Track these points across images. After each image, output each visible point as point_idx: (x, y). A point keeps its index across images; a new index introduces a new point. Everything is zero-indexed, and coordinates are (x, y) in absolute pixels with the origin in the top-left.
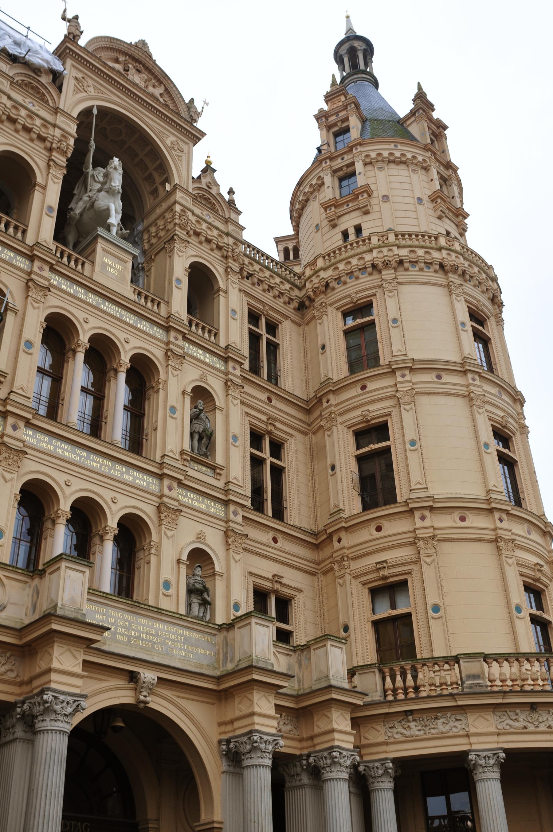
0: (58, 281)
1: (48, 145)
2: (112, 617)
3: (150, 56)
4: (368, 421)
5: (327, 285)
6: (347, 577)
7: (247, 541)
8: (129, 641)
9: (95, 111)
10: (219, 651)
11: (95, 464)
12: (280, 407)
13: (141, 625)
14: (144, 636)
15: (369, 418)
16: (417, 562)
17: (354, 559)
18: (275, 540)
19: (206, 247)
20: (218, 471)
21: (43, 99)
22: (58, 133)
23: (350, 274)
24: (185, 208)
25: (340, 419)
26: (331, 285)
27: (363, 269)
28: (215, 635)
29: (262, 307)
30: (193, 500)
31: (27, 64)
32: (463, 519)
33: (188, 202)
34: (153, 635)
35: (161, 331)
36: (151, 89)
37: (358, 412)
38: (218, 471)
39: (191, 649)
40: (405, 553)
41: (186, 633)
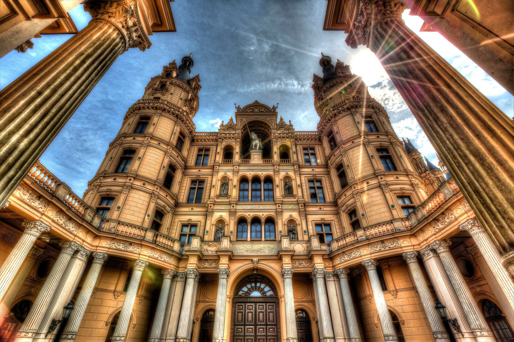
3: (259, 103)
5: (322, 131)
16: (356, 202)
19: (284, 140)
22: (236, 135)
24: (274, 133)
36: (261, 110)
37: (334, 163)
40: (352, 201)
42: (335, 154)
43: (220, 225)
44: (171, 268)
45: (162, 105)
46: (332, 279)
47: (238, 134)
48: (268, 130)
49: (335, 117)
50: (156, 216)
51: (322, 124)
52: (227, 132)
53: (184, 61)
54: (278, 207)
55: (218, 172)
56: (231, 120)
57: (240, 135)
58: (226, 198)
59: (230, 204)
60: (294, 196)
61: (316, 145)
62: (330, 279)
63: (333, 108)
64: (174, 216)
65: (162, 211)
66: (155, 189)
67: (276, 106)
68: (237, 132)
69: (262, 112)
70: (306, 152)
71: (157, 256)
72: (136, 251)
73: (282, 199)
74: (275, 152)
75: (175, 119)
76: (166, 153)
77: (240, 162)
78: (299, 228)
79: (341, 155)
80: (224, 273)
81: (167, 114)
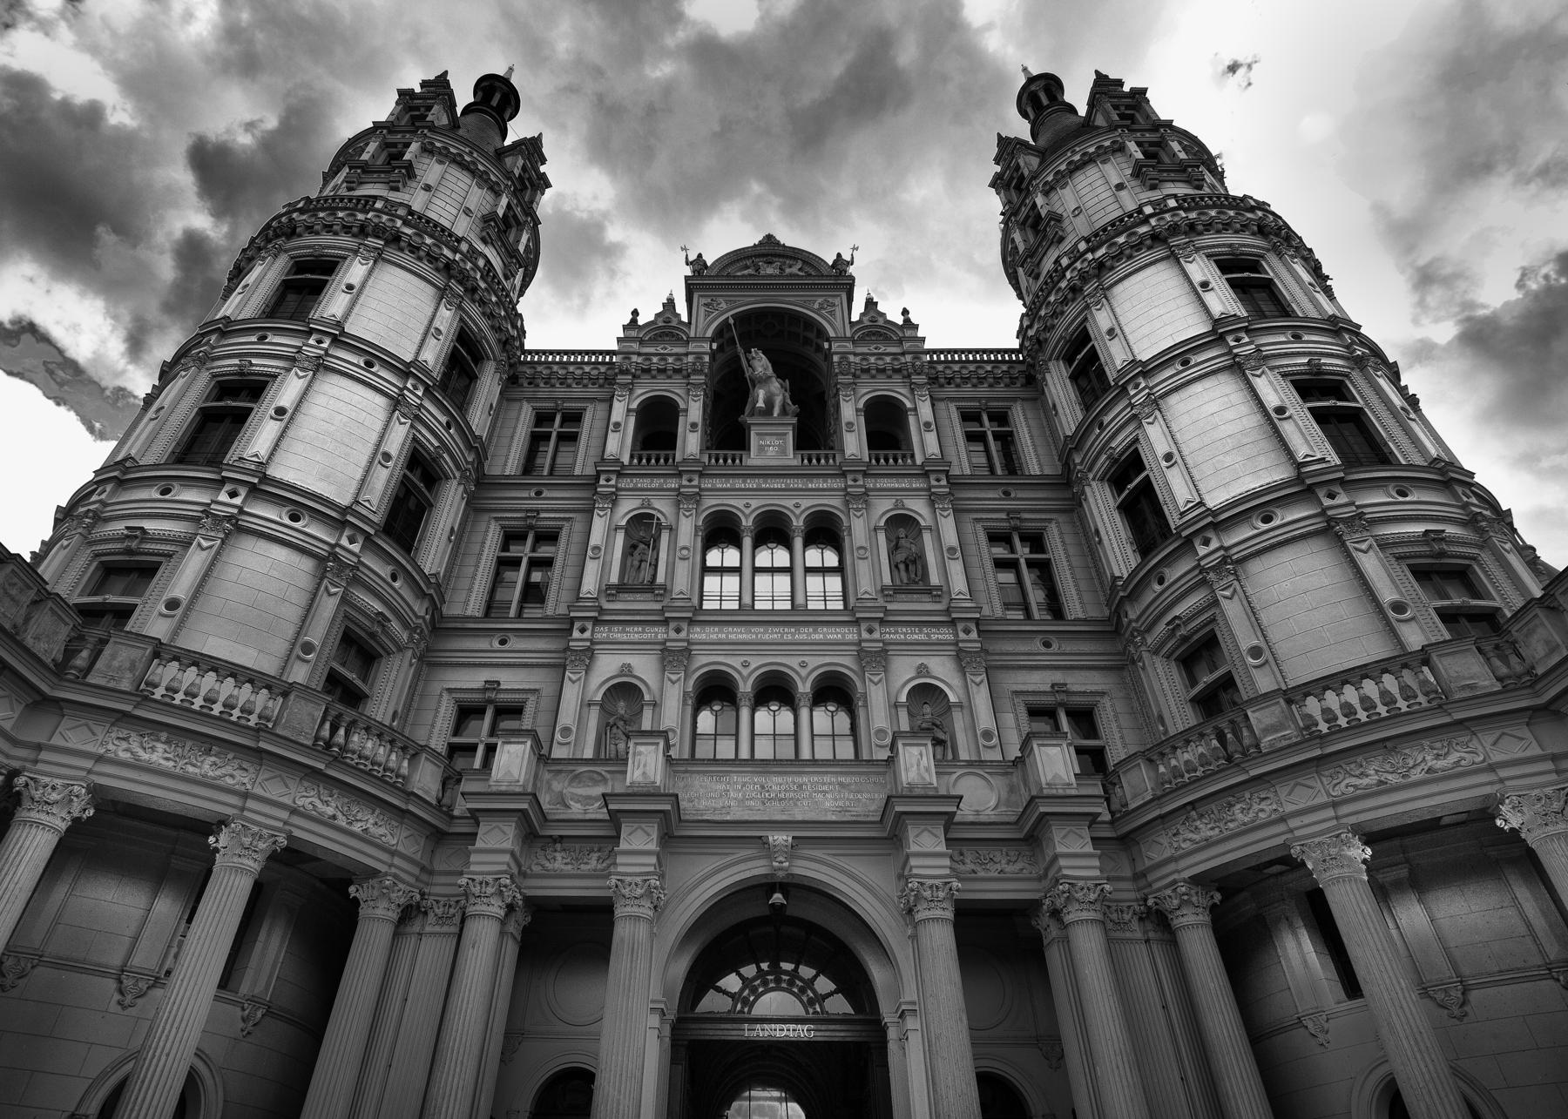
1: (685, 373)
5: (1039, 342)
7: (990, 658)
9: (731, 321)
22: (691, 358)
24: (844, 355)
28: (884, 773)
30: (905, 634)
32: (1267, 519)
33: (849, 346)
36: (788, 271)
39: (851, 797)
41: (842, 779)
43: (622, 707)
44: (393, 870)
45: (385, 218)
47: (699, 356)
48: (819, 348)
52: (651, 350)
53: (483, 89)
54: (865, 635)
56: (670, 304)
57: (707, 359)
58: (649, 596)
59: (666, 622)
60: (930, 591)
61: (1014, 399)
65: (373, 635)
67: (846, 257)
68: (692, 347)
69: (792, 276)
71: (330, 811)
72: (229, 781)
73: (881, 602)
74: (850, 424)
77: (706, 460)
78: (959, 721)
80: (639, 891)
81: (406, 258)
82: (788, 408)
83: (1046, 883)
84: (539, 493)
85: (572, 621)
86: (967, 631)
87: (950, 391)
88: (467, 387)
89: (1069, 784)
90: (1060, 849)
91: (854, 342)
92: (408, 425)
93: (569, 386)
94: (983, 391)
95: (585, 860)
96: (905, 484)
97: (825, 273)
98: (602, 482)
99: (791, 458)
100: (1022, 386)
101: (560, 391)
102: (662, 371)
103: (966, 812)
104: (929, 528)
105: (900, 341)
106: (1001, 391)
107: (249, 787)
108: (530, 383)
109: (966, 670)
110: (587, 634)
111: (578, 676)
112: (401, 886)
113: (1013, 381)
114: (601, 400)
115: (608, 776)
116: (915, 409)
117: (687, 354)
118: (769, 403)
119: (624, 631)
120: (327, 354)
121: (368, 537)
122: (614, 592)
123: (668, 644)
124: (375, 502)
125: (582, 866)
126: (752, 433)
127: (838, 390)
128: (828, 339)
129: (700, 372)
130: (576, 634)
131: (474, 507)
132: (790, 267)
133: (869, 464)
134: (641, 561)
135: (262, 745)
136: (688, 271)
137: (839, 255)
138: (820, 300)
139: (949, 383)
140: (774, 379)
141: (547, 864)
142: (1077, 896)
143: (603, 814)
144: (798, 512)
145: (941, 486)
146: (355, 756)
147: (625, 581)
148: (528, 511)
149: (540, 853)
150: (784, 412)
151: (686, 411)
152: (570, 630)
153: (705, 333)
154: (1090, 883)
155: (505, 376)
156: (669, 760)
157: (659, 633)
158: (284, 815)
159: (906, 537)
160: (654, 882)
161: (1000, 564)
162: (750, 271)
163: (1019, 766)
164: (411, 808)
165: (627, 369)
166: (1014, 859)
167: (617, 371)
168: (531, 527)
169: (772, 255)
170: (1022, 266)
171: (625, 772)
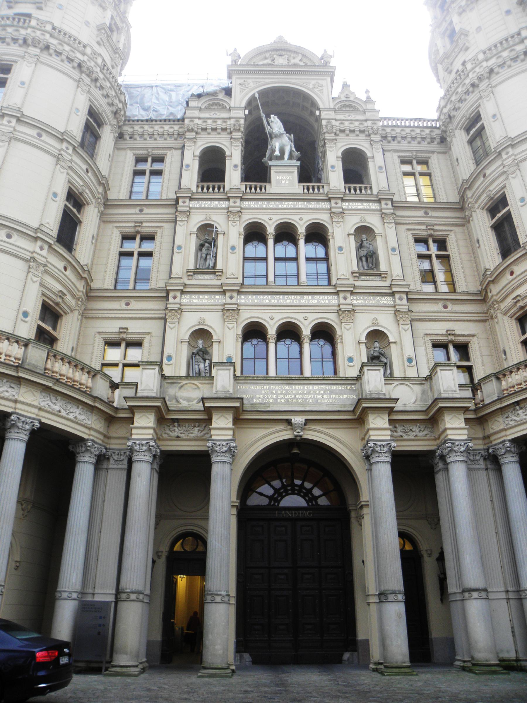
0: (248, 204)
1: (229, 131)
2: (273, 389)
4: (492, 198)
5: (450, 117)
6: (499, 315)
7: (413, 314)
8: (288, 401)
9: (257, 96)
10: (359, 393)
11: (289, 301)
12: (436, 215)
13: (296, 390)
14: (298, 396)
15: (492, 196)
17: (502, 301)
18: (445, 307)
19: (352, 136)
20: (383, 275)
21: (224, 107)
22: (232, 121)
23: (461, 101)
24: (329, 120)
25: (476, 206)
26: (451, 115)
27: (467, 93)
28: (355, 384)
29: (411, 154)
30: (365, 300)
31: (208, 94)
33: (332, 115)
34: (305, 394)
35: (326, 203)
36: (293, 61)
37: (484, 196)
38: (383, 275)
41: (332, 387)
42: (488, 172)
43: (200, 343)
44: (91, 438)
46: (483, 466)
47: (237, 119)
48: (312, 113)
49: (489, 78)
50: (42, 318)
51: (453, 98)
52: (207, 115)
54: (342, 301)
55: (188, 213)
57: (242, 121)
58: (212, 276)
59: (224, 292)
61: (433, 152)
62: (478, 466)
63: (484, 53)
64: (84, 320)
65: (57, 304)
66: (38, 250)
67: (330, 53)
68: (234, 113)
69: (295, 65)
70: (407, 168)
71: (57, 408)
74: (333, 167)
75: (76, 74)
76: (58, 159)
78: (394, 352)
79: (505, 172)
80: (225, 449)
82: (293, 153)
83: (438, 442)
84: (141, 211)
85: (168, 292)
86: (401, 299)
87: (394, 145)
88: (95, 143)
89: (455, 391)
90: (448, 425)
91: (335, 111)
92: (65, 173)
93: (155, 139)
94: (414, 146)
95: (191, 432)
96: (365, 206)
97: (317, 64)
98: (180, 203)
99: (298, 188)
100: (438, 144)
101: (150, 143)
102: (214, 129)
103: (399, 406)
104: (381, 235)
105: (364, 112)
106: (425, 146)
107: (16, 397)
108: (131, 138)
109: (400, 322)
110: (177, 300)
111: (174, 325)
112: (96, 445)
113: (432, 140)
114: (176, 149)
115: (200, 385)
116: (373, 157)
117: (230, 118)
118: (282, 151)
119: (199, 298)
120: (15, 130)
121: (50, 246)
122: (192, 274)
123: (226, 306)
124: (52, 224)
125: (190, 435)
126: (272, 171)
127: (325, 143)
128: (319, 109)
129: (239, 130)
130: (171, 300)
131: (104, 219)
132: (294, 58)
133: (345, 193)
134: (207, 254)
135: (21, 375)
136: (229, 61)
137: (325, 51)
138: (313, 82)
139: (394, 140)
140: (285, 135)
141: (171, 433)
142: (455, 449)
143: (200, 406)
144: (301, 223)
145: (387, 207)
146: (65, 378)
147: (198, 267)
148: (135, 222)
149: (166, 428)
150: (291, 157)
151: (231, 156)
152: (167, 297)
153: (240, 104)
154: (462, 443)
155: (116, 135)
156: (236, 378)
157: (220, 299)
158: (36, 411)
159: (367, 240)
160: (233, 444)
161: (421, 257)
162: (268, 61)
163: (429, 380)
164: (97, 405)
165: (192, 129)
166: (422, 429)
167: (186, 129)
168: (138, 232)
169: (282, 50)
170: (441, 64)
171: (213, 383)
